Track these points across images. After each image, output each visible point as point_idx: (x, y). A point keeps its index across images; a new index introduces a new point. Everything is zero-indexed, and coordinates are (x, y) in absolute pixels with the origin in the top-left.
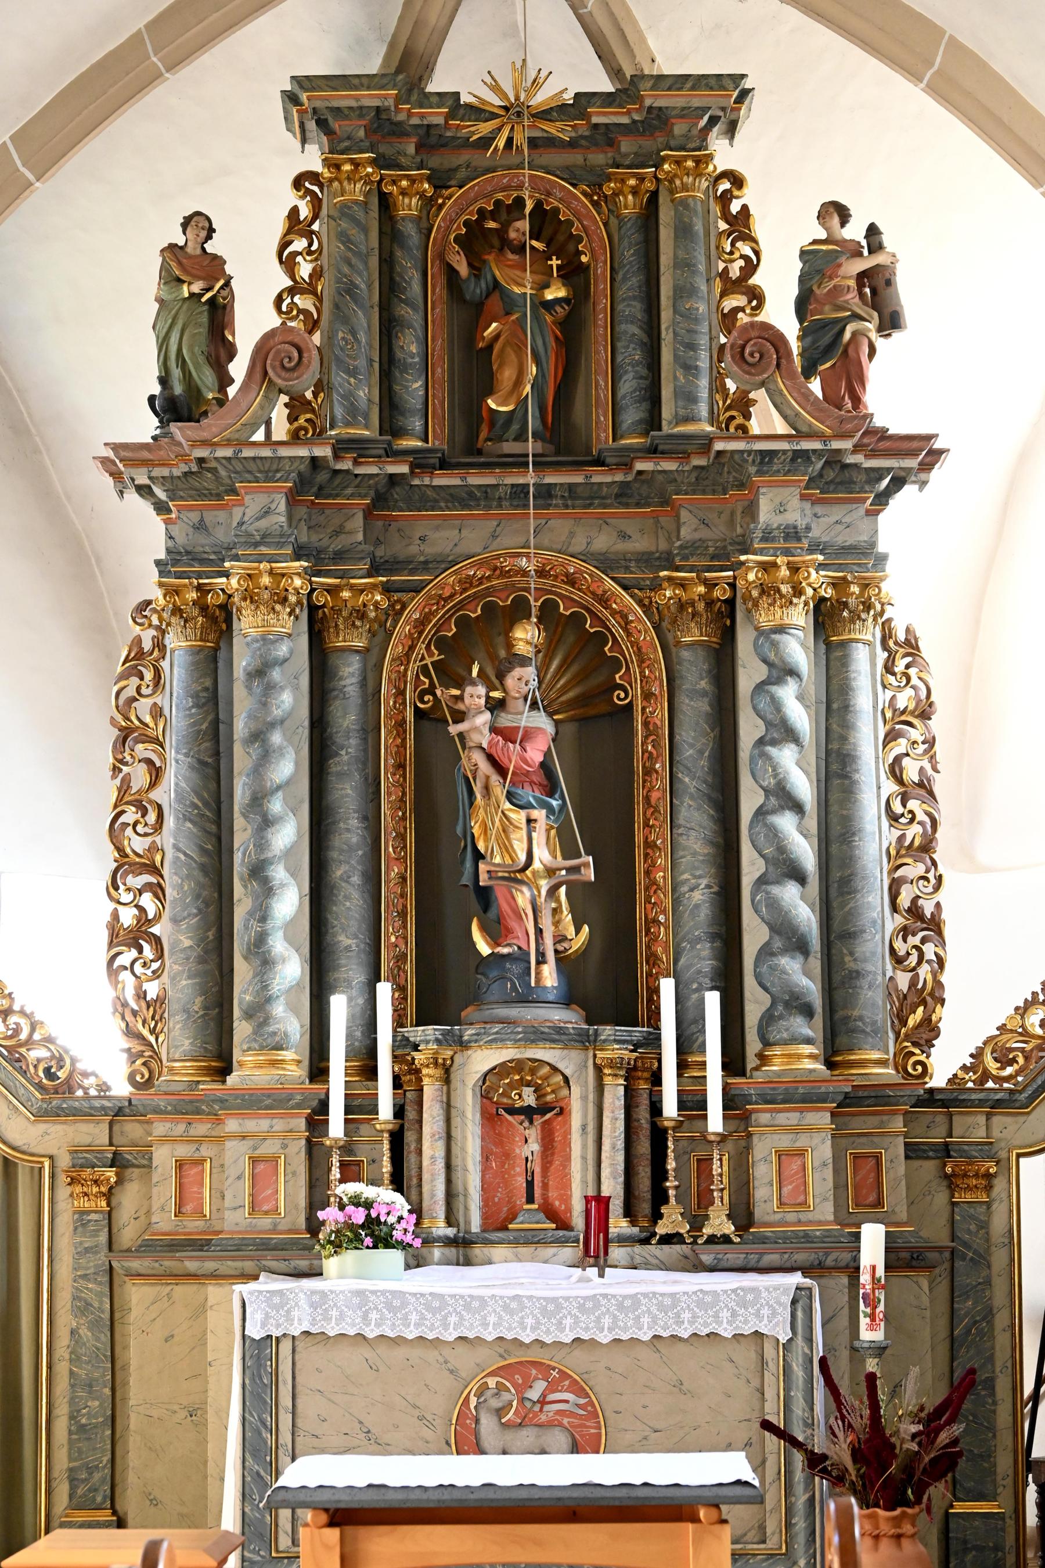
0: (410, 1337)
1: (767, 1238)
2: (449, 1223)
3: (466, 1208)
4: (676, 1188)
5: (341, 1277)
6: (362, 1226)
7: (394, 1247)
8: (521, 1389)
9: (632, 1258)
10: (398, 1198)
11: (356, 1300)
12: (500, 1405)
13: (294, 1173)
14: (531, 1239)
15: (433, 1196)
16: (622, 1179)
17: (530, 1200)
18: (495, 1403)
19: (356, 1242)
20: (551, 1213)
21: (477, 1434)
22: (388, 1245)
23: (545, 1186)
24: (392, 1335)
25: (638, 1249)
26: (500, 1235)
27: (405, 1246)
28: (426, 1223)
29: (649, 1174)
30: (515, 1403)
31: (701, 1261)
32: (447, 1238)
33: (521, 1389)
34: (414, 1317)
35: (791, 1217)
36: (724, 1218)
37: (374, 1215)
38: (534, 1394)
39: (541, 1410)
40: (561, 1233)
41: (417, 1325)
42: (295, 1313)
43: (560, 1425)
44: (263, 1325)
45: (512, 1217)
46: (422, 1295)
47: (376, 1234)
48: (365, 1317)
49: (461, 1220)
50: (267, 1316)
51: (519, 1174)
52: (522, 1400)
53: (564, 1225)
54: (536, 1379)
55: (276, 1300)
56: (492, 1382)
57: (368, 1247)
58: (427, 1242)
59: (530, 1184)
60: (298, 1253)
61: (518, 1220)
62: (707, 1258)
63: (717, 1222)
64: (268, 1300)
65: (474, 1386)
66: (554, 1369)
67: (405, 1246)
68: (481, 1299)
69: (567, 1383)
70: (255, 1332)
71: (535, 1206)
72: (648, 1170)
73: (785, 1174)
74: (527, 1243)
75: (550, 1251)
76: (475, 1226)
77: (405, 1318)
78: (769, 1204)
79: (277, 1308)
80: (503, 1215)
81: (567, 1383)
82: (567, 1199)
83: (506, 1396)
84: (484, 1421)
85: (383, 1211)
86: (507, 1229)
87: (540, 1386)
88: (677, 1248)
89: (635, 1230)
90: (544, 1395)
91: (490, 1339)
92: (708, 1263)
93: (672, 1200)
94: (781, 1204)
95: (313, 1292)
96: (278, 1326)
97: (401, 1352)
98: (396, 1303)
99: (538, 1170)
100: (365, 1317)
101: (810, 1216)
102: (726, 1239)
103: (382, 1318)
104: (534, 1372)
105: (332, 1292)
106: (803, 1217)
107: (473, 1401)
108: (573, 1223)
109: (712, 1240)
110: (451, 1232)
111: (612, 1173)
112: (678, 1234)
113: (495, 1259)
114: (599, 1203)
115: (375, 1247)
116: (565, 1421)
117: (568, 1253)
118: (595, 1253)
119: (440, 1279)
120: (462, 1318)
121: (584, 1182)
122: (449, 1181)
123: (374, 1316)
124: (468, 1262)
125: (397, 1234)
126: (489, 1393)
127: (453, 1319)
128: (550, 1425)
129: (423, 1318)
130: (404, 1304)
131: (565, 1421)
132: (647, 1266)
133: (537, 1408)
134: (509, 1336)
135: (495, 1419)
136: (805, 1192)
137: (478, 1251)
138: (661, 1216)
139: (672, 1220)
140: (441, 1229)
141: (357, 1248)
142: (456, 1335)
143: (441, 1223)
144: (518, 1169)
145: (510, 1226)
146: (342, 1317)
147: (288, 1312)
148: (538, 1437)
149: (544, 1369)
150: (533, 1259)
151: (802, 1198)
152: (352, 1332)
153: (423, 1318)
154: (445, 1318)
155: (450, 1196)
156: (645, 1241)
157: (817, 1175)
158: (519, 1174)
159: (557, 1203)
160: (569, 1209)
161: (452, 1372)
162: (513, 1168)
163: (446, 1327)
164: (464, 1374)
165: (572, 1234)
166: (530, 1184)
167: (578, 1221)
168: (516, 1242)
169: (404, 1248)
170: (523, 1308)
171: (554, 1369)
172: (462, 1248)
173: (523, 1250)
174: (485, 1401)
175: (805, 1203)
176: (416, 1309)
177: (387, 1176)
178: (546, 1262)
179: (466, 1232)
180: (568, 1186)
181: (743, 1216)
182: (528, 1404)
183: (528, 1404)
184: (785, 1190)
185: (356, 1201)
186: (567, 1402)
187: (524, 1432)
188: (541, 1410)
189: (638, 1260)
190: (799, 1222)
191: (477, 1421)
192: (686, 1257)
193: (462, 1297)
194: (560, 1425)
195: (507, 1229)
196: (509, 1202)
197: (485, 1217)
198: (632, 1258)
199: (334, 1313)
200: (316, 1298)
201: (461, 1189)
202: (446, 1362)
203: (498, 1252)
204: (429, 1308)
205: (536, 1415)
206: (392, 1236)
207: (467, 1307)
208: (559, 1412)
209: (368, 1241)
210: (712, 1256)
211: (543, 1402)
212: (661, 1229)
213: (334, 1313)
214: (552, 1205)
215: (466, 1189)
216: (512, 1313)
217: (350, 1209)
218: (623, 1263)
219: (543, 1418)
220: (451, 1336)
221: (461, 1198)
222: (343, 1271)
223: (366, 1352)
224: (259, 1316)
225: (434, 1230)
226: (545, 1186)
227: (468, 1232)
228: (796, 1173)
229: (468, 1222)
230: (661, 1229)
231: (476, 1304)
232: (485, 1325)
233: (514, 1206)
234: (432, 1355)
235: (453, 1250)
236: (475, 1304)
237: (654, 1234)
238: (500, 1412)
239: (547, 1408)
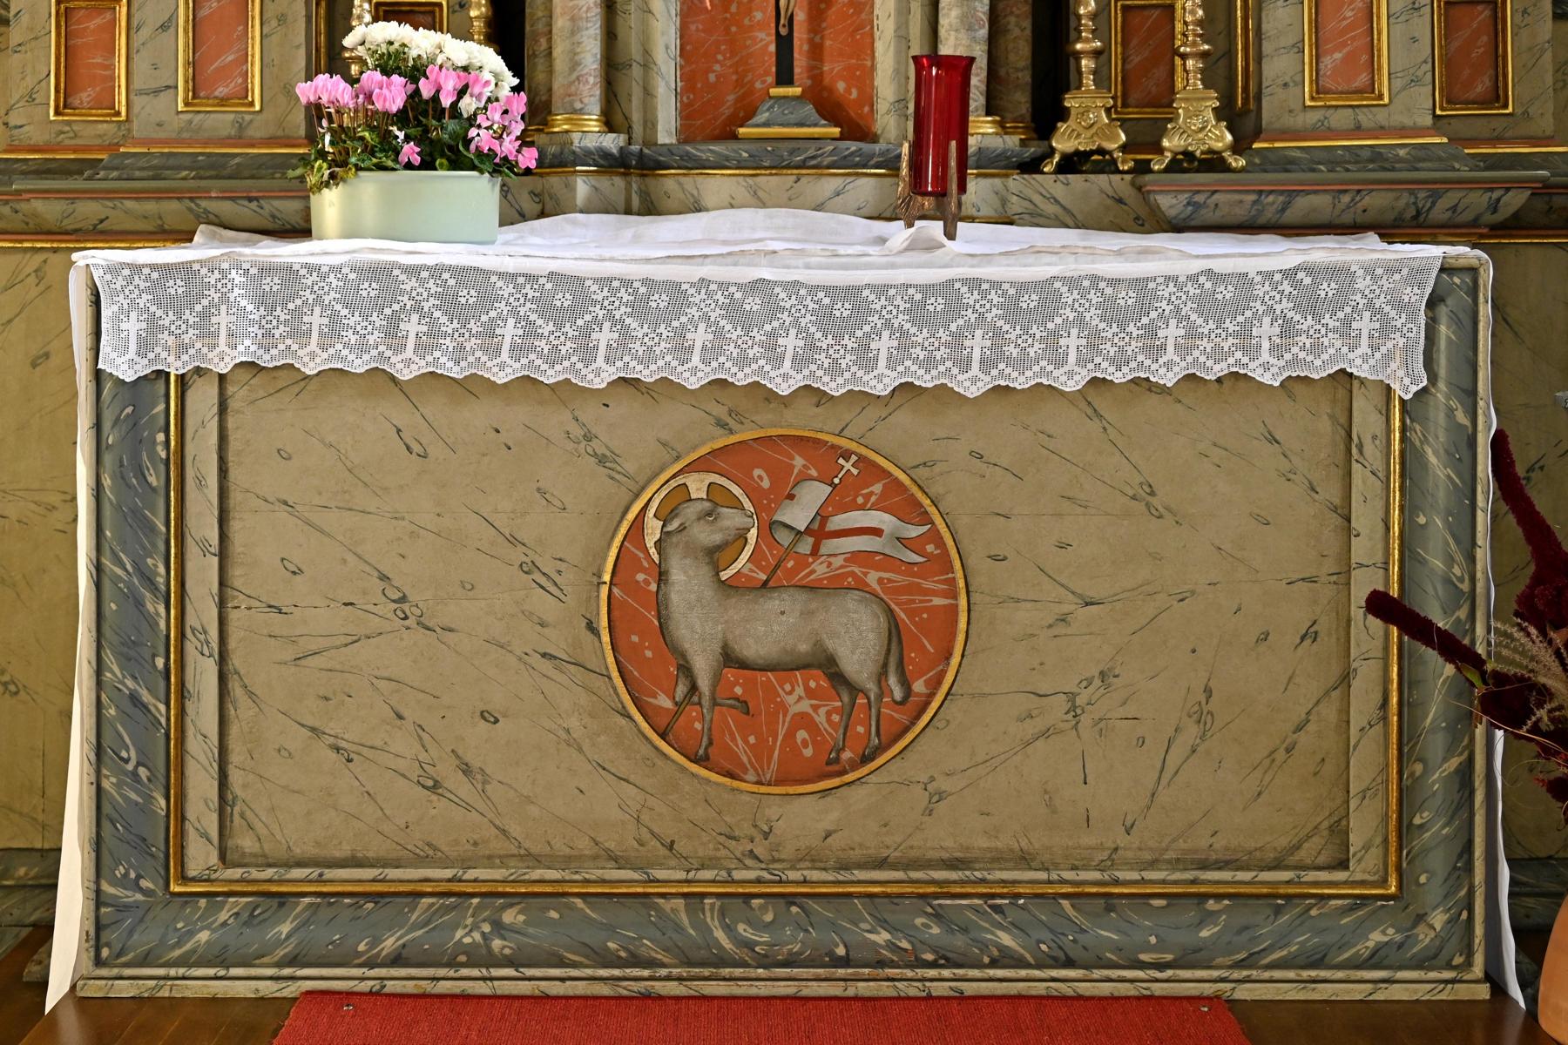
0: (501, 378)
1: (1293, 161)
2: (609, 125)
3: (648, 93)
4: (1097, 54)
5: (349, 234)
6: (401, 118)
7: (473, 168)
8: (767, 503)
9: (1004, 202)
10: (490, 60)
11: (369, 290)
12: (717, 538)
13: (282, 19)
14: (786, 161)
15: (575, 65)
16: (983, 32)
17: (785, 76)
18: (707, 535)
19: (381, 155)
20: (830, 110)
21: (660, 605)
22: (457, 163)
23: (816, 51)
24: (456, 373)
25: (1017, 182)
26: (719, 148)
27: (498, 166)
28: (560, 124)
29: (1028, 32)
30: (754, 531)
31: (1155, 210)
32: (605, 154)
33: (767, 503)
34: (510, 332)
35: (1341, 119)
36: (1210, 115)
37: (426, 91)
38: (798, 515)
39: (815, 552)
40: (853, 146)
41: (517, 351)
42: (223, 320)
43: (861, 586)
44: (144, 346)
45: (746, 114)
46: (531, 278)
47: (431, 134)
48: (392, 331)
49: (636, 117)
50: (153, 326)
51: (761, 26)
52: (770, 527)
53: (857, 130)
54: (804, 478)
55: (176, 287)
56: (697, 485)
57: (409, 166)
58: (559, 161)
59: (785, 44)
60: (264, 192)
61: (757, 120)
62: (1170, 203)
63: (1196, 123)
64: (155, 288)
65: (654, 494)
66: (846, 455)
67: (498, 166)
68: (673, 287)
69: (877, 488)
70: (123, 365)
71: (796, 91)
72: (1027, 24)
73: (1330, 26)
74: (779, 166)
75: (829, 185)
76: (666, 134)
77: (490, 331)
78: (1294, 90)
79: (177, 306)
80: (726, 110)
81: (877, 488)
82: (864, 76)
83: (731, 519)
84: (677, 575)
85: (450, 84)
86: (734, 137)
87: (813, 495)
88: (1102, 180)
89: (1012, 141)
90: (822, 516)
91: (693, 384)
92: (1172, 213)
93: (1089, 81)
94: (1319, 91)
95: (266, 270)
96: (182, 348)
97: (479, 415)
98: (468, 296)
99: (800, 17)
100: (392, 331)
101: (1381, 117)
102: (1213, 163)
103: (434, 333)
104: (799, 462)
105: (311, 268)
106: (1365, 118)
107: (653, 529)
108: (878, 128)
109: (1185, 162)
110: (612, 142)
111: (963, 18)
112: (1101, 151)
113: (708, 200)
114: (940, 82)
115: (427, 165)
116: (873, 578)
117: (866, 187)
118: (931, 183)
119: (582, 245)
120: (626, 333)
121: (902, 37)
122: (610, 36)
123: (412, 327)
124: (650, 208)
125: (481, 138)
126: (691, 511)
127: (604, 337)
128: (835, 586)
129: (531, 332)
130: (488, 299)
131: (873, 578)
132: (1036, 219)
133: (805, 546)
134: (741, 378)
135: (706, 570)
136: (1372, 67)
137: (671, 183)
138: (1063, 114)
139: (1088, 120)
140: (590, 133)
141: (381, 168)
142: (610, 374)
143: (593, 124)
144: (758, 16)
145: (742, 130)
146: (334, 330)
147: (205, 315)
148: (807, 614)
149: (823, 454)
150: (791, 202)
151: (1362, 80)
152: (359, 366)
153: (531, 332)
154: (586, 332)
155: (612, 66)
156: (1031, 167)
157: (1398, 29)
158: (761, 26)
159: (841, 86)
160: (869, 98)
161: (602, 460)
162: (749, 12)
163: (587, 352)
164: (630, 467)
165: (877, 148)
166: (785, 44)
167: (892, 123)
168: (754, 164)
169: (496, 171)
170: (774, 310)
171: (846, 455)
172: (639, 179)
173: (770, 182)
174: (682, 529)
175: (1370, 88)
176: (514, 312)
177: (478, 25)
178: (819, 208)
179: (645, 144)
180: (864, 46)
181: (1240, 116)
182: (784, 538)
183: (784, 538)
184: (1328, 62)
185: (391, 62)
186: (876, 532)
187: (774, 603)
188: (815, 552)
189: (1016, 205)
190: (1358, 131)
191: (662, 576)
192: (1120, 201)
193: (627, 283)
194: (861, 586)
195: (735, 137)
196: (739, 83)
197: (687, 113)
198: (1004, 202)
199: (316, 320)
200: (272, 283)
201: (635, 52)
202: (588, 437)
203: (716, 184)
204: (545, 308)
205: (802, 563)
206: (467, 142)
207: (639, 307)
208: (855, 557)
209: (410, 151)
210: (1183, 198)
211: (819, 531)
212: (1064, 142)
213: (316, 320)
214: (831, 90)
215: (647, 52)
216: (746, 322)
217: (372, 77)
218: (986, 211)
219: (820, 569)
220: (600, 375)
221: (636, 71)
222: (352, 225)
223: (401, 414)
224: (133, 326)
225: (576, 137)
226: (816, 51)
227: (650, 142)
228: (1351, 27)
229: (650, 123)
230: (1064, 142)
231: (660, 301)
232: (683, 351)
233: (751, 91)
234: (556, 421)
235: (619, 182)
236: (659, 301)
237: (1052, 151)
238: (715, 556)
239: (829, 546)
